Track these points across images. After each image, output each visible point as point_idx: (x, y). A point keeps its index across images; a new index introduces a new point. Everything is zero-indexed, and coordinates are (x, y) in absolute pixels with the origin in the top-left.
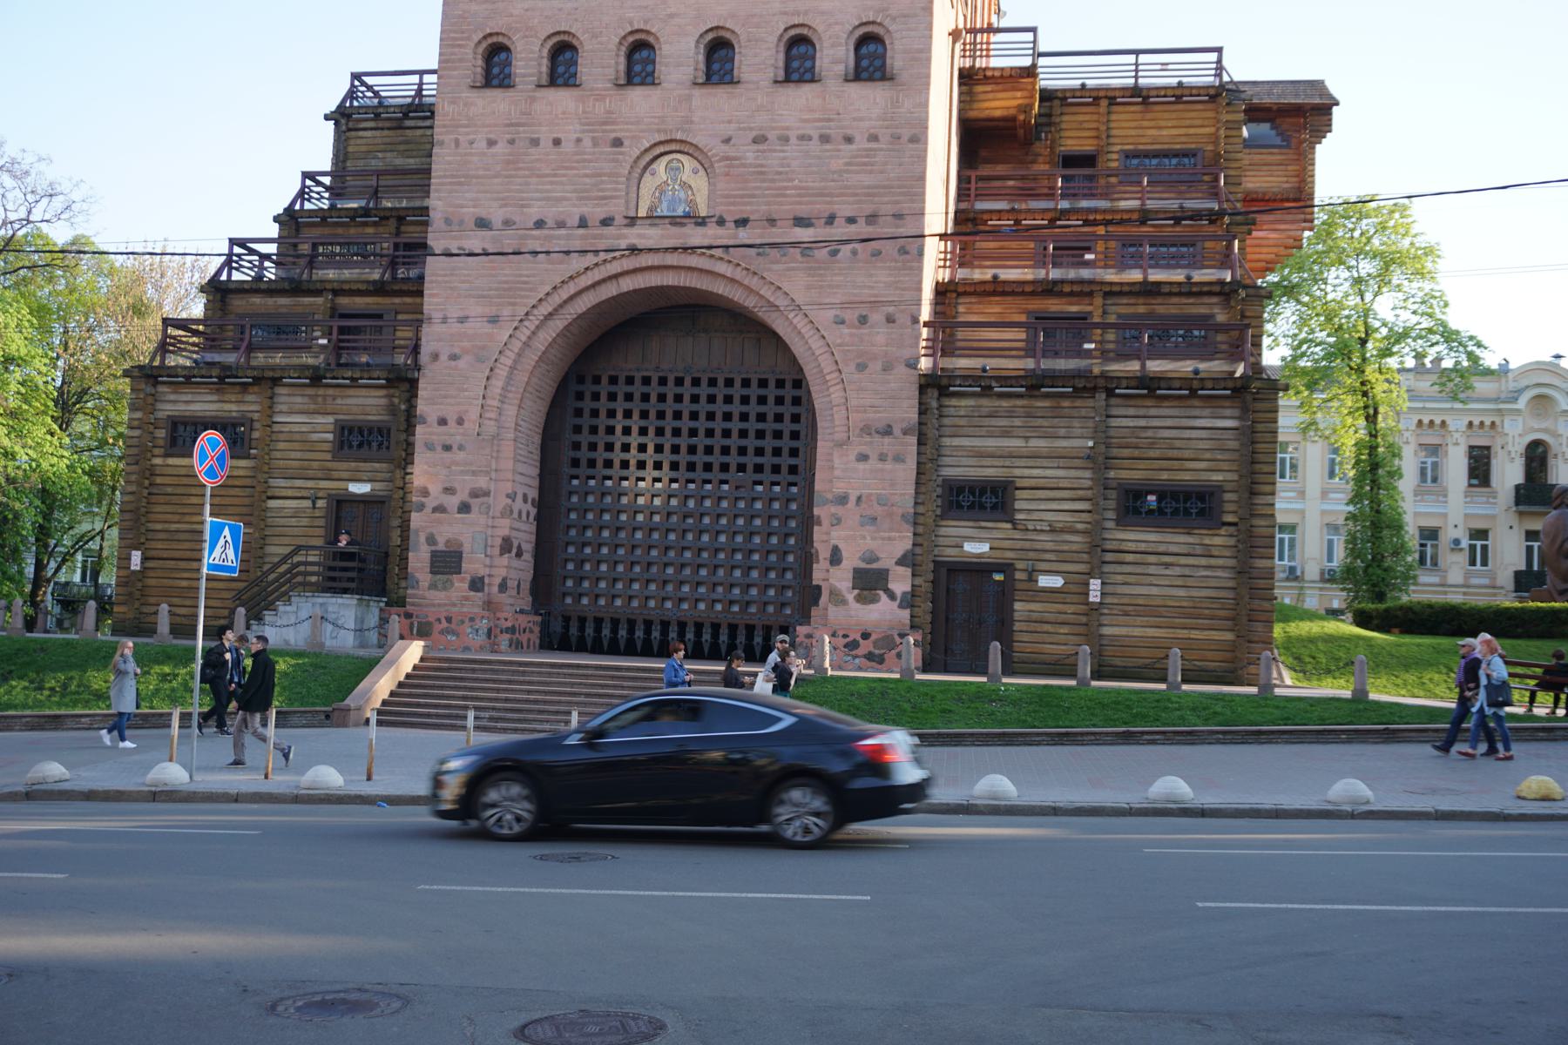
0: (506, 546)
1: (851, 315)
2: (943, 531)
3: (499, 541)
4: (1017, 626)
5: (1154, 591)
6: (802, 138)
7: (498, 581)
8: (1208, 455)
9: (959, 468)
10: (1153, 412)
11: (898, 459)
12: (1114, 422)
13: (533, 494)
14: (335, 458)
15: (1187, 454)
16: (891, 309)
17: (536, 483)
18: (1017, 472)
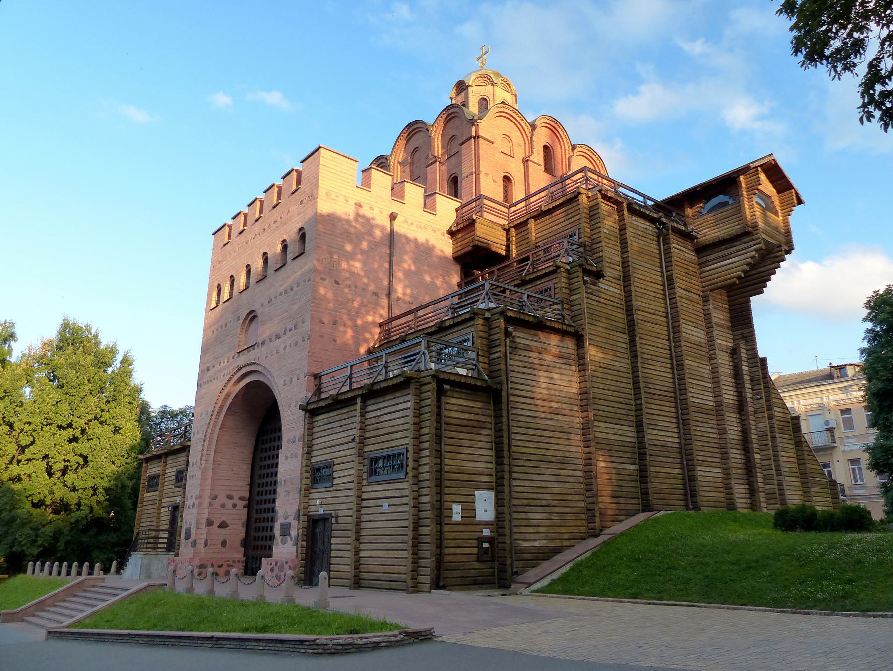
0: (210, 523)
1: (288, 380)
2: (312, 496)
3: (204, 521)
4: (333, 554)
5: (381, 524)
6: (281, 294)
7: (203, 541)
8: (401, 428)
9: (319, 458)
10: (382, 405)
11: (296, 457)
12: (368, 415)
13: (247, 495)
14: (176, 487)
15: (394, 429)
16: (298, 372)
17: (248, 488)
18: (335, 455)
